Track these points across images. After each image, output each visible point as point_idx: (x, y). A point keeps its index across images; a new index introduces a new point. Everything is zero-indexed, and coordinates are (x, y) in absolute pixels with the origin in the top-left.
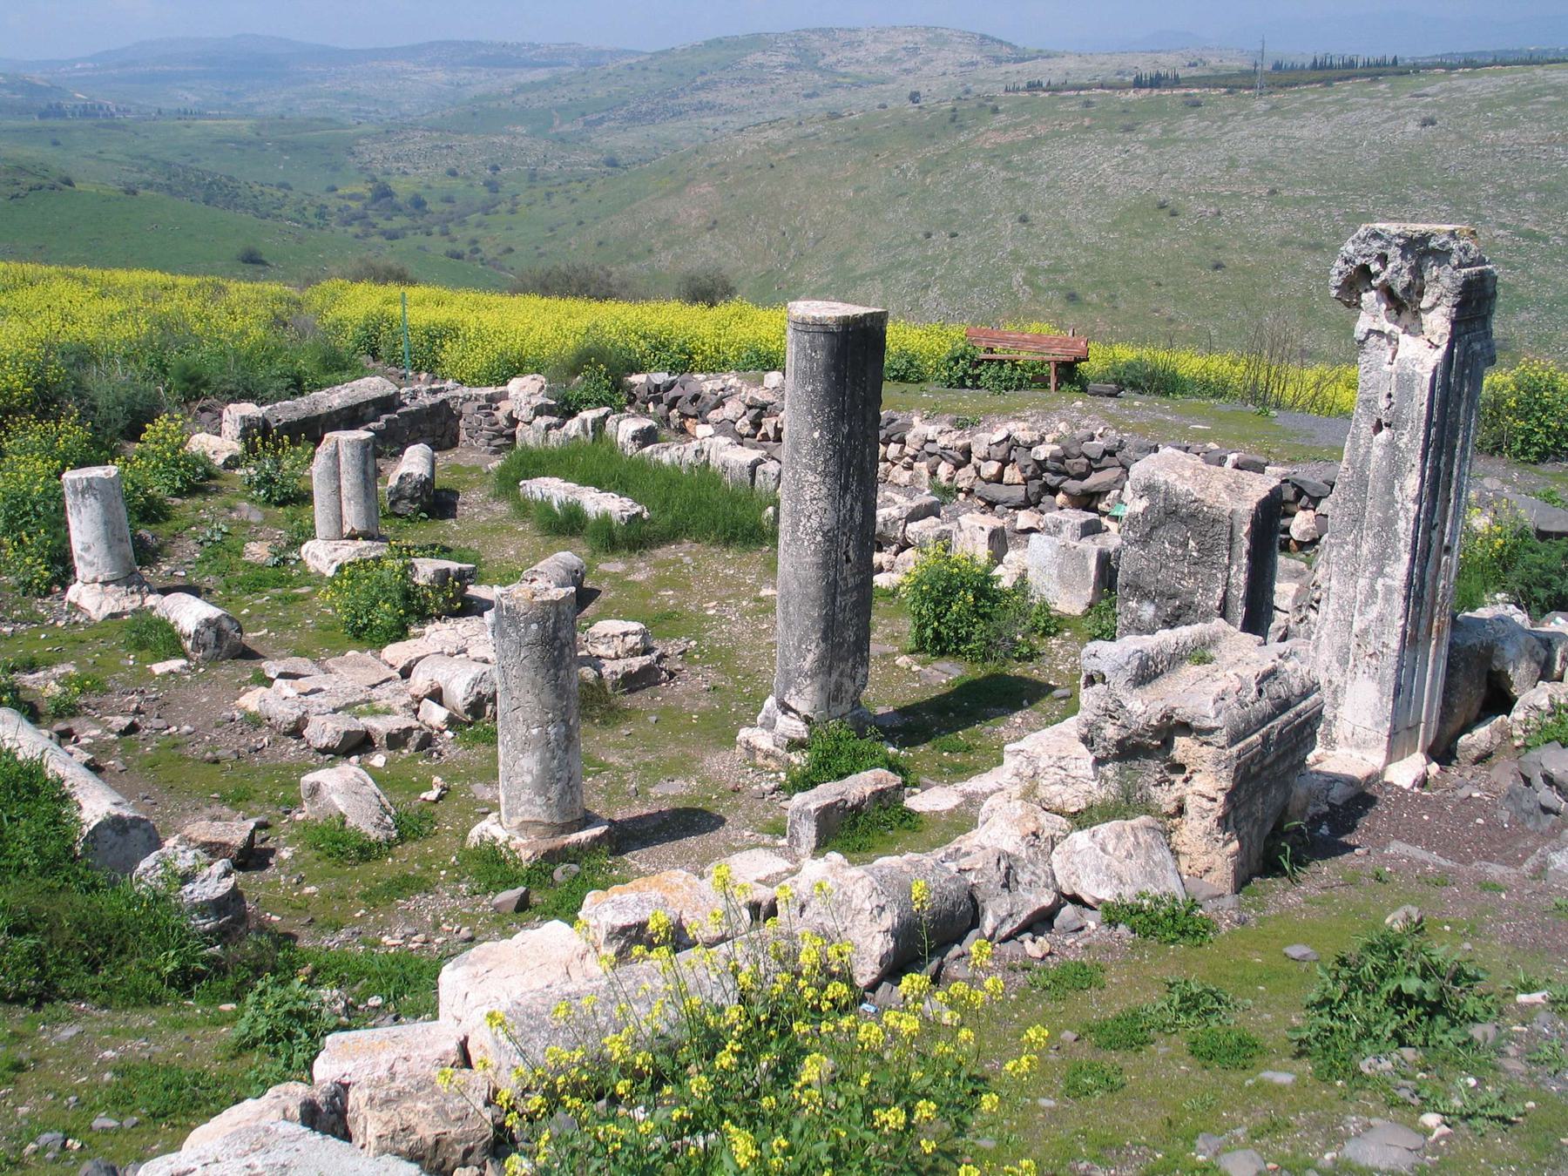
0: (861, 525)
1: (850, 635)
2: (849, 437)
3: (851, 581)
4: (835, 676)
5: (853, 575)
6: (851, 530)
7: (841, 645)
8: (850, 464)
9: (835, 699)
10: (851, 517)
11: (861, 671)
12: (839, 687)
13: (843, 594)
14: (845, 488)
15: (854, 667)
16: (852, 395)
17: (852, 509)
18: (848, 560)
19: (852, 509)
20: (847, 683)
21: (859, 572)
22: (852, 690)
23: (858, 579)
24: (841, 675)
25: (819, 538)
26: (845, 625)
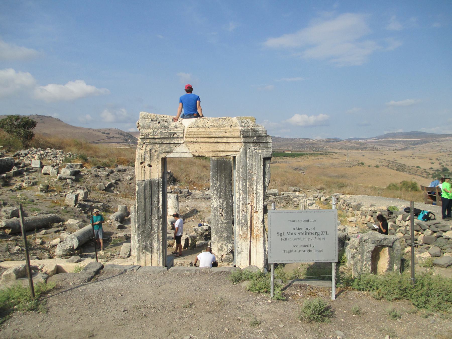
0: (227, 208)
1: (225, 235)
2: (220, 185)
3: (224, 221)
4: (220, 244)
7: (222, 237)
8: (220, 192)
10: (222, 205)
12: (221, 247)
13: (222, 224)
14: (220, 198)
15: (227, 243)
16: (220, 176)
17: (222, 203)
18: (222, 216)
19: (222, 203)
20: (224, 247)
21: (226, 219)
22: (226, 249)
23: (226, 221)
24: (222, 244)
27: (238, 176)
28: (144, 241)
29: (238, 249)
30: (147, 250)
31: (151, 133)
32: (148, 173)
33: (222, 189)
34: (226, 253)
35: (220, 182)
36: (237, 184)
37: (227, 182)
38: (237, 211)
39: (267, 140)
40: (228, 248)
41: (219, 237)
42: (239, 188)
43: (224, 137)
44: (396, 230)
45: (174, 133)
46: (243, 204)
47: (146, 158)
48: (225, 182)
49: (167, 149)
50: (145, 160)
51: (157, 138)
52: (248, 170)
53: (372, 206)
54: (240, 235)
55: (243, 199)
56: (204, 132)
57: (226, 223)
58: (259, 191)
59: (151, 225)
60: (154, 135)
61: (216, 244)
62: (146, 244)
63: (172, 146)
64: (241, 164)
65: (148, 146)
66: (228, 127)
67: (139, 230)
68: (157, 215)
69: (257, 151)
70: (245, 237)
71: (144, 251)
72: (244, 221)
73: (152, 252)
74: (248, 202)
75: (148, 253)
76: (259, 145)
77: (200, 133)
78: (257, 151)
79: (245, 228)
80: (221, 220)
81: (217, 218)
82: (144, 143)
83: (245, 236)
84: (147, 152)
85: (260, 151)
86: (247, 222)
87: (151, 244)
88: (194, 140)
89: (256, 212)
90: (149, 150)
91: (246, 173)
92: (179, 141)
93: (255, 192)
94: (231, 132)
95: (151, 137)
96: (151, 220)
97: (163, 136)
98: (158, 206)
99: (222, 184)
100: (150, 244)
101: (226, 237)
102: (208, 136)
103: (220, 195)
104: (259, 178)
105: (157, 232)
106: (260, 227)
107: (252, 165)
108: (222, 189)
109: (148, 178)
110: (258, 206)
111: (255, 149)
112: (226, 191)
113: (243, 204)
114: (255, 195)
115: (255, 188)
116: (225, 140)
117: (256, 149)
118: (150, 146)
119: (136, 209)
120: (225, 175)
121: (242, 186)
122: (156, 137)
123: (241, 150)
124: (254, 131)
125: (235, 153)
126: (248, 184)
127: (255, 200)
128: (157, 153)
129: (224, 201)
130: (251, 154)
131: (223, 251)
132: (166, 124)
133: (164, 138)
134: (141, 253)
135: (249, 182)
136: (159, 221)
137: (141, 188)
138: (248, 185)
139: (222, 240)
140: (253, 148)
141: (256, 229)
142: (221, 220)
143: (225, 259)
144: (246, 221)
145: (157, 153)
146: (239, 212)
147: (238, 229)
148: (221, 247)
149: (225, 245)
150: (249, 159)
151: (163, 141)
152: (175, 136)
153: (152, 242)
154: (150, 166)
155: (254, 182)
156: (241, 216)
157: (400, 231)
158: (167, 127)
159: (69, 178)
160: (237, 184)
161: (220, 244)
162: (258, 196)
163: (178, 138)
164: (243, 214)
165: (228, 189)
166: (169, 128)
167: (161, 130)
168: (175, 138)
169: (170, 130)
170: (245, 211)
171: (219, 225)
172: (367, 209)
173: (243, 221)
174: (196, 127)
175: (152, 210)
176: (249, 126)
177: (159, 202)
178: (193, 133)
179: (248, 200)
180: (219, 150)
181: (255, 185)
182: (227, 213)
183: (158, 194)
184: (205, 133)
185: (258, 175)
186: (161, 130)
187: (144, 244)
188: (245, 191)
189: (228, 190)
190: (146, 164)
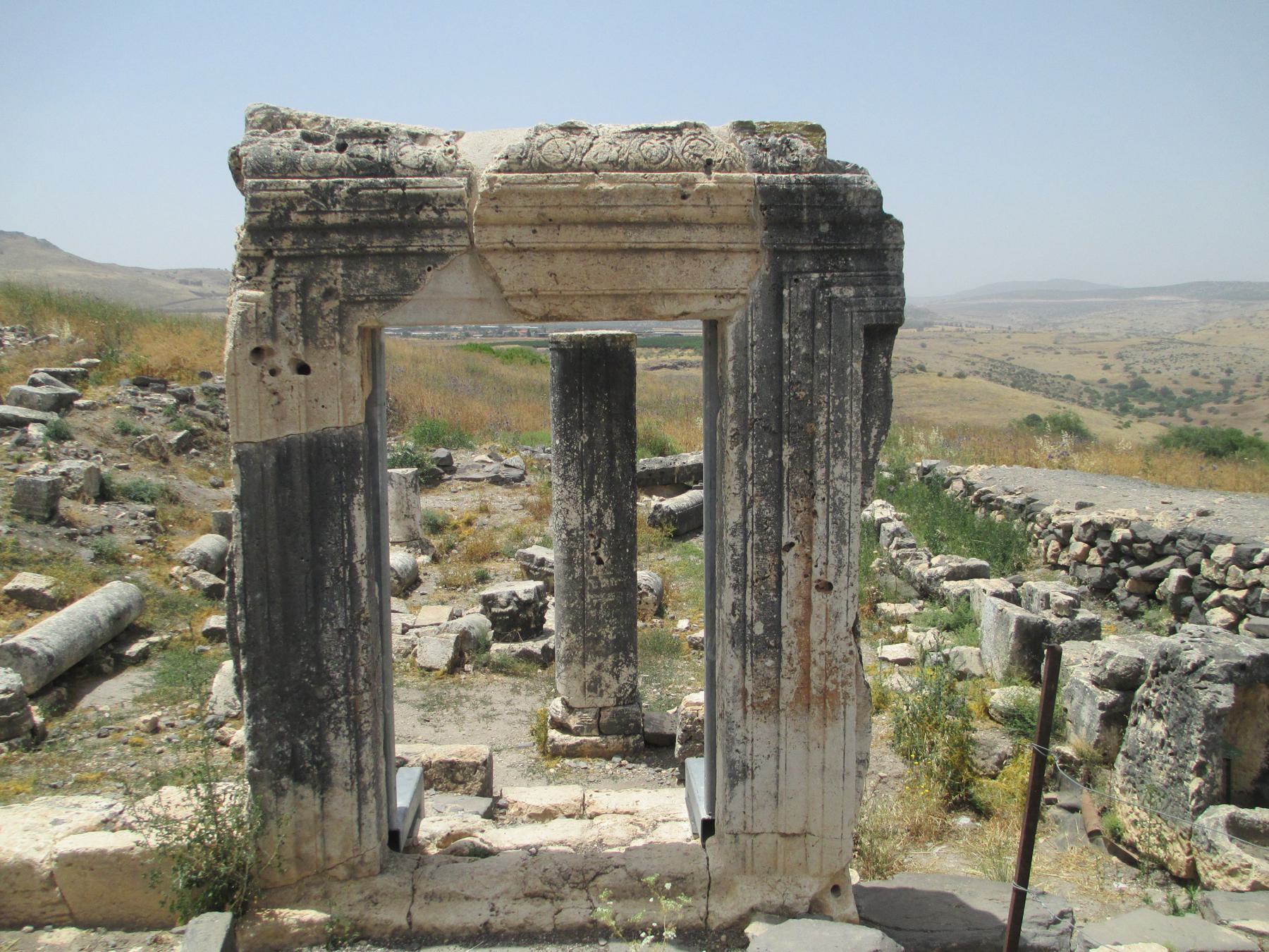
0: (616, 531)
1: (609, 633)
2: (590, 445)
3: (605, 583)
4: (590, 668)
5: (608, 577)
6: (600, 533)
7: (596, 640)
8: (592, 472)
9: (594, 690)
10: (600, 522)
11: (626, 672)
12: (597, 681)
13: (597, 592)
14: (589, 494)
15: (616, 664)
16: (591, 408)
17: (600, 515)
18: (600, 562)
19: (600, 515)
20: (607, 677)
23: (614, 582)
24: (599, 667)
25: (564, 536)
26: (599, 623)
27: (741, 413)
28: (280, 738)
29: (736, 756)
30: (299, 778)
31: (301, 200)
32: (292, 401)
33: (599, 458)
34: (612, 701)
35: (589, 433)
36: (733, 455)
37: (617, 432)
38: (728, 582)
39: (880, 237)
40: (622, 680)
41: (585, 640)
42: (743, 472)
43: (672, 222)
44: (1200, 598)
45: (423, 201)
46: (760, 549)
47: (281, 328)
48: (610, 433)
49: (386, 283)
50: (273, 334)
51: (336, 228)
52: (791, 383)
53: (1081, 506)
54: (745, 692)
55: (760, 524)
56: (574, 192)
57: (612, 589)
58: (839, 484)
59: (318, 659)
60: (319, 211)
61: (575, 668)
62: (294, 747)
63: (409, 267)
64: (754, 356)
65: (290, 266)
66: (693, 168)
67: (252, 689)
68: (340, 610)
69: (835, 291)
70: (767, 704)
71: (285, 781)
72: (766, 629)
73: (323, 784)
74: (785, 541)
75: (306, 791)
76: (841, 262)
77: (550, 202)
78: (835, 291)
79: (770, 663)
80: (596, 578)
81: (578, 571)
82: (269, 253)
83: (767, 696)
84: (284, 295)
85: (850, 292)
86: (780, 635)
87: (320, 747)
88: (524, 237)
89: (827, 587)
90: (292, 286)
91: (779, 400)
92: (446, 239)
93: (821, 491)
94: (706, 193)
95: (304, 219)
96: (317, 633)
97: (362, 218)
98: (345, 564)
99: (599, 440)
100: (311, 746)
101: (614, 642)
102: (593, 215)
103: (591, 482)
104: (840, 424)
105: (346, 691)
106: (839, 656)
107: (809, 358)
108: (599, 458)
109: (296, 428)
110: (832, 559)
111: (824, 285)
112: (612, 468)
113: (760, 549)
114: (819, 507)
115: (820, 474)
116: (676, 236)
117: (829, 284)
118: (294, 268)
119: (238, 581)
120: (608, 405)
121: (759, 462)
122: (330, 219)
123: (756, 285)
124: (822, 194)
125: (726, 304)
126: (787, 451)
127: (820, 529)
128: (334, 304)
129: (606, 506)
130: (806, 307)
131: (601, 695)
132: (377, 153)
133: (369, 228)
134: (269, 794)
135: (793, 443)
136: (352, 638)
137: (257, 476)
138: (785, 460)
139: (597, 654)
140: (816, 276)
141: (822, 664)
142: (596, 578)
143: (610, 724)
144: (775, 629)
145: (334, 304)
146: (740, 586)
147: (737, 665)
148: (597, 681)
149: (612, 672)
150: (793, 329)
151: (362, 239)
152: (427, 214)
153: (322, 738)
154: (303, 369)
155: (820, 441)
156: (752, 605)
157: (1220, 603)
158: (385, 168)
159: (35, 421)
160: (733, 455)
161: (590, 668)
162: (837, 509)
163: (440, 225)
164: (760, 597)
165: (621, 458)
166: (393, 174)
167: (353, 182)
168: (430, 225)
169: (397, 185)
170: (772, 579)
171: (588, 597)
172: (1067, 520)
173: (759, 629)
174: (530, 169)
175: (317, 582)
176: (796, 167)
177: (352, 546)
178: (519, 202)
179: (785, 531)
180: (647, 286)
181: (821, 455)
182: (615, 551)
183: (346, 508)
184: (581, 201)
185: (841, 408)
186: (353, 182)
187: (285, 747)
188: (774, 489)
189: (623, 467)
190: (282, 358)
